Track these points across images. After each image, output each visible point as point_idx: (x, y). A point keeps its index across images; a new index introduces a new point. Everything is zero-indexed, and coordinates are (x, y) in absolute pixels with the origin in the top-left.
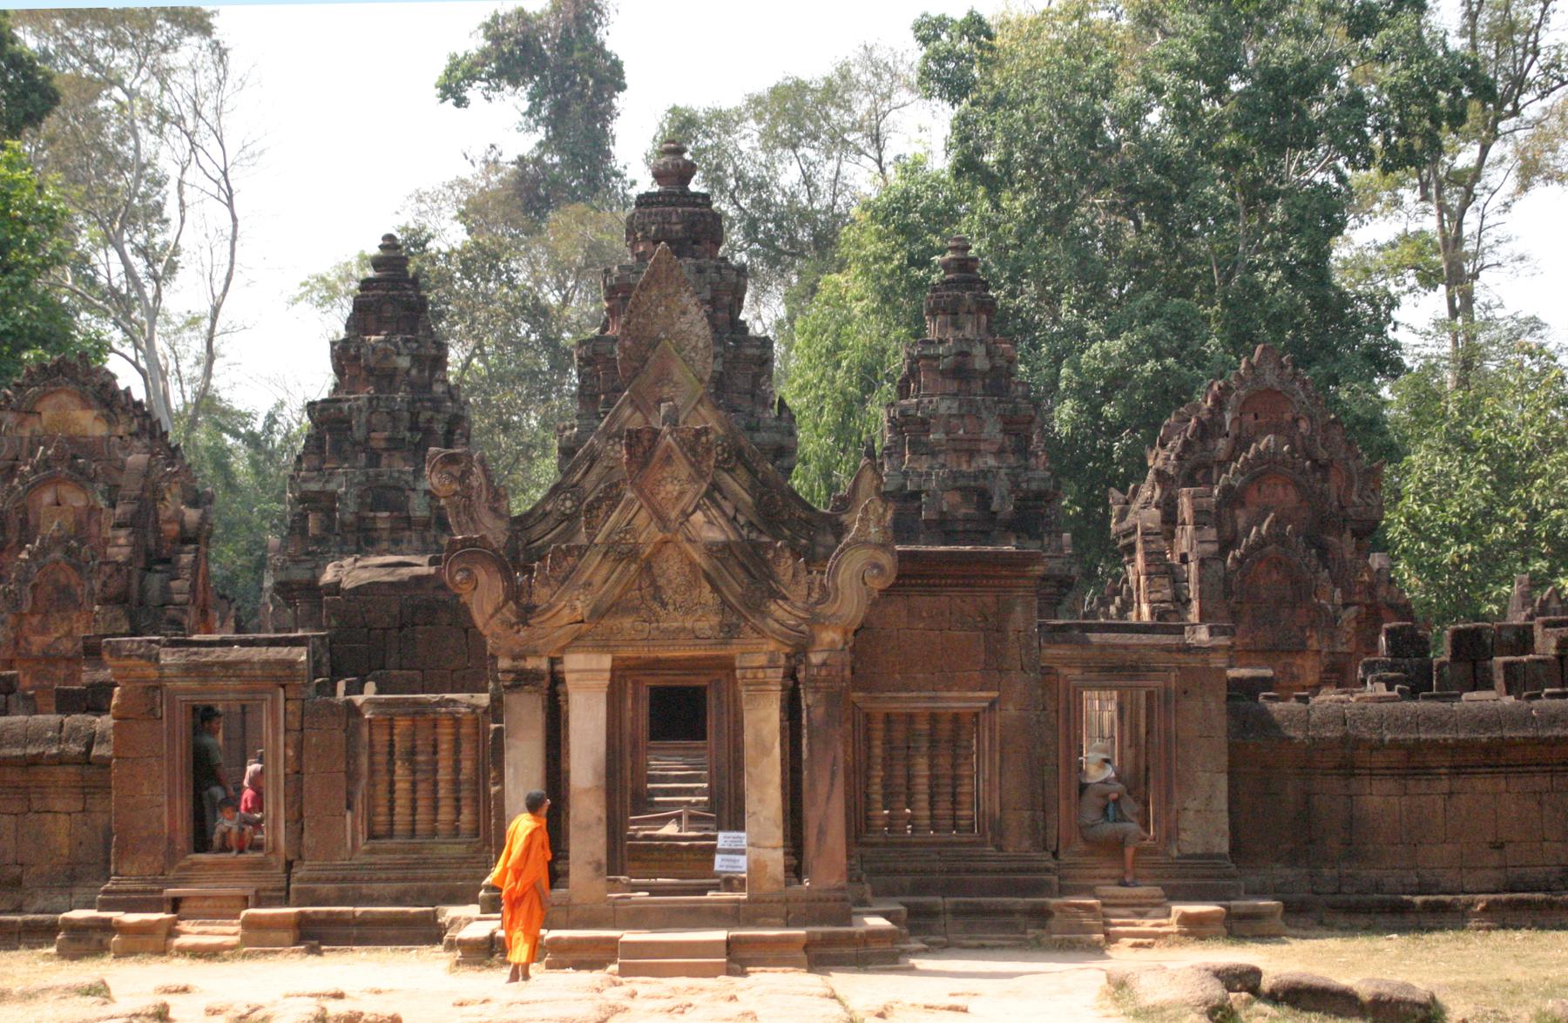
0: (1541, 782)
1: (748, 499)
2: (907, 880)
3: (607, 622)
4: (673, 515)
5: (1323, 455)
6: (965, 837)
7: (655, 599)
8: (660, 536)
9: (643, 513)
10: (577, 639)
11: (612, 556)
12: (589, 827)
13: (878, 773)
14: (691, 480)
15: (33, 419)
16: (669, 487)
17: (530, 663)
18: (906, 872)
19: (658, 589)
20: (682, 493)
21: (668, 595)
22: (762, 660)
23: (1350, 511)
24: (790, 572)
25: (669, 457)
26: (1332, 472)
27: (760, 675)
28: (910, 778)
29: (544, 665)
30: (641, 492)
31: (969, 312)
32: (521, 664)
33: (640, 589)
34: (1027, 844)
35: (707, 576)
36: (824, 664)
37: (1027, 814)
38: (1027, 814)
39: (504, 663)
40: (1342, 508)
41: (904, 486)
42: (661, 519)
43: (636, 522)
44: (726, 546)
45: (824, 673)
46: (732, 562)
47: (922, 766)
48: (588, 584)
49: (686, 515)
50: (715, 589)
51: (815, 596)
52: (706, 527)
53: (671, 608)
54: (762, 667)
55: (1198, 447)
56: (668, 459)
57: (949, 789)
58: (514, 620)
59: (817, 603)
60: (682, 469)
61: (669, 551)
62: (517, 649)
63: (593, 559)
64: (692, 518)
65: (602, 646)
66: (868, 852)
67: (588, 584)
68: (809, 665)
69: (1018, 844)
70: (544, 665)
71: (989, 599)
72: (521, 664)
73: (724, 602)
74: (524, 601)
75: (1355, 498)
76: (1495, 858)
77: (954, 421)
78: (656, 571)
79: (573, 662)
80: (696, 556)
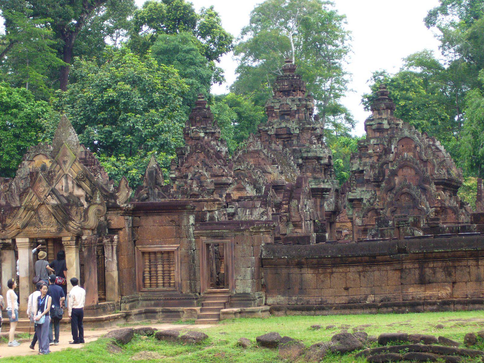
0: (360, 268)
1: (89, 189)
2: (153, 302)
3: (27, 229)
4: (42, 197)
5: (425, 158)
6: (171, 289)
9: (35, 197)
10: (18, 234)
11: (26, 209)
12: (24, 288)
13: (148, 269)
14: (47, 186)
15: (32, 163)
16: (41, 189)
17: (7, 241)
18: (153, 300)
19: (40, 218)
20: (44, 190)
22: (69, 238)
23: (435, 176)
26: (428, 164)
28: (157, 271)
29: (10, 241)
30: (34, 190)
31: (383, 109)
32: (4, 241)
34: (189, 291)
35: (53, 215)
36: (86, 239)
37: (189, 281)
38: (189, 281)
40: (432, 175)
41: (359, 169)
42: (40, 199)
46: (59, 210)
47: (160, 268)
48: (20, 218)
50: (55, 218)
55: (384, 157)
56: (40, 181)
57: (152, 275)
60: (44, 183)
61: (43, 207)
62: (3, 237)
63: (21, 211)
65: (25, 236)
66: (143, 294)
67: (20, 218)
68: (81, 240)
69: (186, 290)
70: (10, 241)
71: (176, 217)
72: (4, 241)
73: (58, 222)
74: (4, 223)
75: (436, 172)
76: (345, 293)
77: (376, 146)
78: (40, 213)
79: (18, 240)
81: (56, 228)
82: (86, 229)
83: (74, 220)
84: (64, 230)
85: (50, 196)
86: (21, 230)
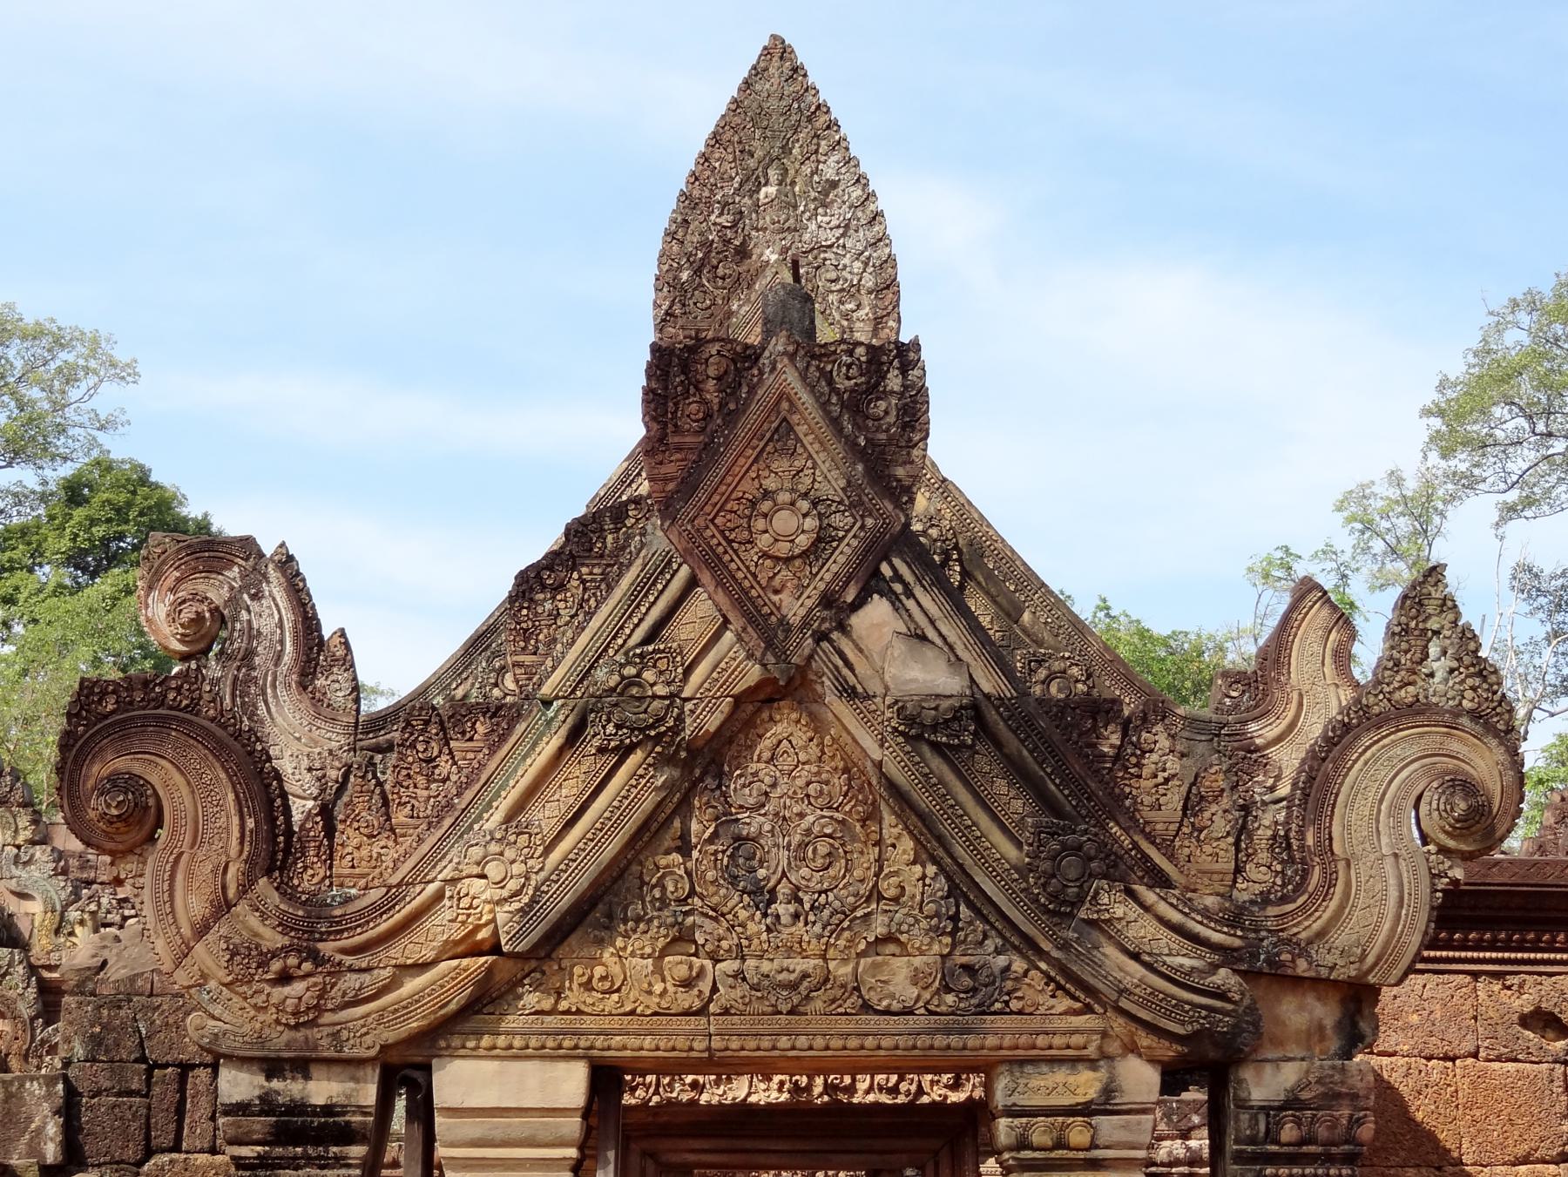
4: (794, 606)
7: (734, 880)
8: (754, 673)
9: (701, 610)
16: (784, 521)
17: (321, 1090)
20: (823, 541)
21: (775, 863)
24: (1173, 800)
25: (785, 430)
27: (1078, 1134)
36: (1292, 1103)
44: (974, 709)
45: (1288, 1133)
46: (984, 762)
49: (836, 610)
51: (1259, 876)
52: (900, 647)
53: (783, 909)
54: (1085, 1111)
58: (273, 938)
59: (1265, 900)
62: (280, 1040)
64: (858, 621)
73: (960, 887)
74: (307, 882)
79: (460, 1081)
81: (927, 953)
82: (1297, 982)
83: (1160, 880)
84: (1035, 990)
85: (878, 611)
86: (507, 969)
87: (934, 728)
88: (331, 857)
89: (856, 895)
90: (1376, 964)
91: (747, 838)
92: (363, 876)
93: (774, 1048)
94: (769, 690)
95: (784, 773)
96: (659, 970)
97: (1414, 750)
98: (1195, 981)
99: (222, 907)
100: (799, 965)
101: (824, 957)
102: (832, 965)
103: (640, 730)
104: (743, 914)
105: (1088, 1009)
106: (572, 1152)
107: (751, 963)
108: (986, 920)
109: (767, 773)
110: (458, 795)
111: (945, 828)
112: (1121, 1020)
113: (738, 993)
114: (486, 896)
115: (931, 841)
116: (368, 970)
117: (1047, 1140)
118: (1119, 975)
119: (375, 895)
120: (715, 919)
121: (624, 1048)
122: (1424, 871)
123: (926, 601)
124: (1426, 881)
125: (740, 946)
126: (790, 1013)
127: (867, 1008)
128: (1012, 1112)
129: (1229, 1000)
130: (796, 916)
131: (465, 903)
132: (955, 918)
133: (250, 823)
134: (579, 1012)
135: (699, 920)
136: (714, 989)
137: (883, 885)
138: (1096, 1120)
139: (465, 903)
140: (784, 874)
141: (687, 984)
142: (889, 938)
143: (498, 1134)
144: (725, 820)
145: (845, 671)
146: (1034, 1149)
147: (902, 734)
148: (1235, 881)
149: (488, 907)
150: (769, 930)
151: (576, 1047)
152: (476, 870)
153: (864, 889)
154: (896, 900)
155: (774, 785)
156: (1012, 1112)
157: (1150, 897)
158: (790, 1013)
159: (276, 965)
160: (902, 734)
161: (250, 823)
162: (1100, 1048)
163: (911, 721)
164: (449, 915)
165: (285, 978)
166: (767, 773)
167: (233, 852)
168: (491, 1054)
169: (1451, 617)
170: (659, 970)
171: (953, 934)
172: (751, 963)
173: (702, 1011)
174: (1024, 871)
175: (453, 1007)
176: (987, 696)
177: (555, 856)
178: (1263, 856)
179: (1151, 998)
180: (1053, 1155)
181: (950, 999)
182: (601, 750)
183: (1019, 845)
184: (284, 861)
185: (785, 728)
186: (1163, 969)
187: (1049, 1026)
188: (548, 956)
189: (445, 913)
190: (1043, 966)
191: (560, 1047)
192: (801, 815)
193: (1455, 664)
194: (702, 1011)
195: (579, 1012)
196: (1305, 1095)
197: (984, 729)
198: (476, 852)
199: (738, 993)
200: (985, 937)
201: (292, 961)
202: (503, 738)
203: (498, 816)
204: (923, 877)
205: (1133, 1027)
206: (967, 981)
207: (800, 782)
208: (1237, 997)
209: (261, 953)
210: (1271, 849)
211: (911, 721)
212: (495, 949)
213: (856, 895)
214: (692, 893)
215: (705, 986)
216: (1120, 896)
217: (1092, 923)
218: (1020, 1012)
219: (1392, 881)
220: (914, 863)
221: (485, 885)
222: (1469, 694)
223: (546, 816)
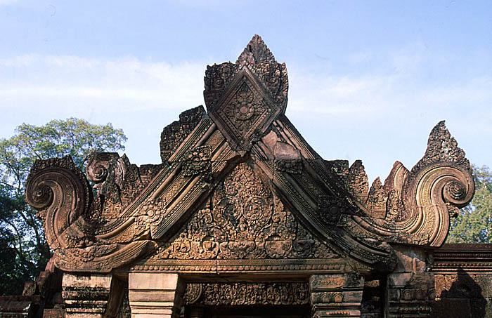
17: (94, 282)
27: (338, 298)
29: (107, 283)
33: (211, 208)
35: (280, 194)
39: (67, 281)
43: (210, 143)
44: (301, 162)
45: (407, 296)
51: (394, 213)
53: (241, 226)
54: (340, 290)
58: (81, 234)
62: (81, 267)
73: (298, 218)
79: (138, 280)
80: (269, 174)
83: (363, 214)
87: (290, 169)
88: (102, 210)
89: (265, 221)
90: (433, 240)
91: (230, 204)
92: (110, 215)
93: (237, 270)
94: (239, 159)
95: (243, 185)
96: (201, 245)
97: (440, 174)
98: (374, 246)
99: (67, 224)
100: (246, 243)
101: (254, 240)
102: (257, 243)
103: (198, 171)
104: (229, 228)
105: (340, 256)
106: (172, 304)
107: (231, 243)
108: (305, 228)
109: (237, 184)
110: (141, 191)
111: (293, 199)
112: (351, 260)
113: (226, 252)
114: (148, 221)
115: (288, 206)
116: (110, 244)
117: (327, 300)
118: (350, 244)
119: (113, 221)
120: (220, 229)
121: (189, 270)
122: (446, 210)
123: (287, 133)
124: (447, 214)
125: (227, 237)
126: (243, 258)
127: (268, 257)
128: (316, 291)
129: (386, 252)
130: (245, 228)
131: (141, 223)
132: (297, 228)
133: (78, 200)
134: (176, 259)
135: (215, 230)
136: (219, 251)
137: (273, 218)
138: (343, 293)
139: (141, 223)
140: (242, 215)
141: (211, 249)
142: (275, 235)
143: (148, 298)
144: (224, 200)
145: (262, 153)
146: (323, 303)
147: (280, 171)
148: (386, 215)
149: (148, 224)
150: (237, 233)
151: (174, 269)
152: (145, 213)
153: (268, 219)
154: (277, 222)
155: (240, 188)
156: (316, 291)
157: (359, 219)
158: (243, 258)
159: (81, 242)
160: (280, 171)
161: (78, 200)
162: (344, 269)
163: (282, 167)
164: (136, 227)
165: (84, 246)
166: (237, 184)
167: (73, 208)
168: (147, 271)
169: (448, 135)
170: (201, 245)
171: (297, 232)
172: (231, 243)
173: (215, 258)
174: (318, 212)
175: (135, 256)
176: (306, 160)
177: (170, 209)
178: (395, 207)
179: (361, 252)
180: (330, 305)
181: (295, 254)
182: (185, 176)
183: (317, 204)
184: (88, 211)
185: (242, 171)
186: (365, 242)
187: (327, 262)
188: (167, 241)
189: (135, 226)
190: (325, 243)
191: (169, 269)
192: (248, 197)
193: (450, 149)
194: (215, 258)
195: (176, 259)
196: (411, 284)
197: (304, 169)
198: (145, 208)
199: (226, 252)
200: (307, 234)
201: (87, 241)
202: (156, 174)
203: (153, 197)
204: (287, 215)
205: (355, 261)
206: (301, 248)
207: (247, 187)
208: (389, 251)
209: (77, 238)
210: (397, 204)
211: (282, 167)
212: (150, 238)
213: (265, 221)
214: (213, 221)
215: (216, 250)
216: (350, 219)
217: (341, 228)
218: (318, 258)
219: (437, 214)
220: (284, 211)
221: (147, 219)
222: (456, 158)
223: (168, 196)
